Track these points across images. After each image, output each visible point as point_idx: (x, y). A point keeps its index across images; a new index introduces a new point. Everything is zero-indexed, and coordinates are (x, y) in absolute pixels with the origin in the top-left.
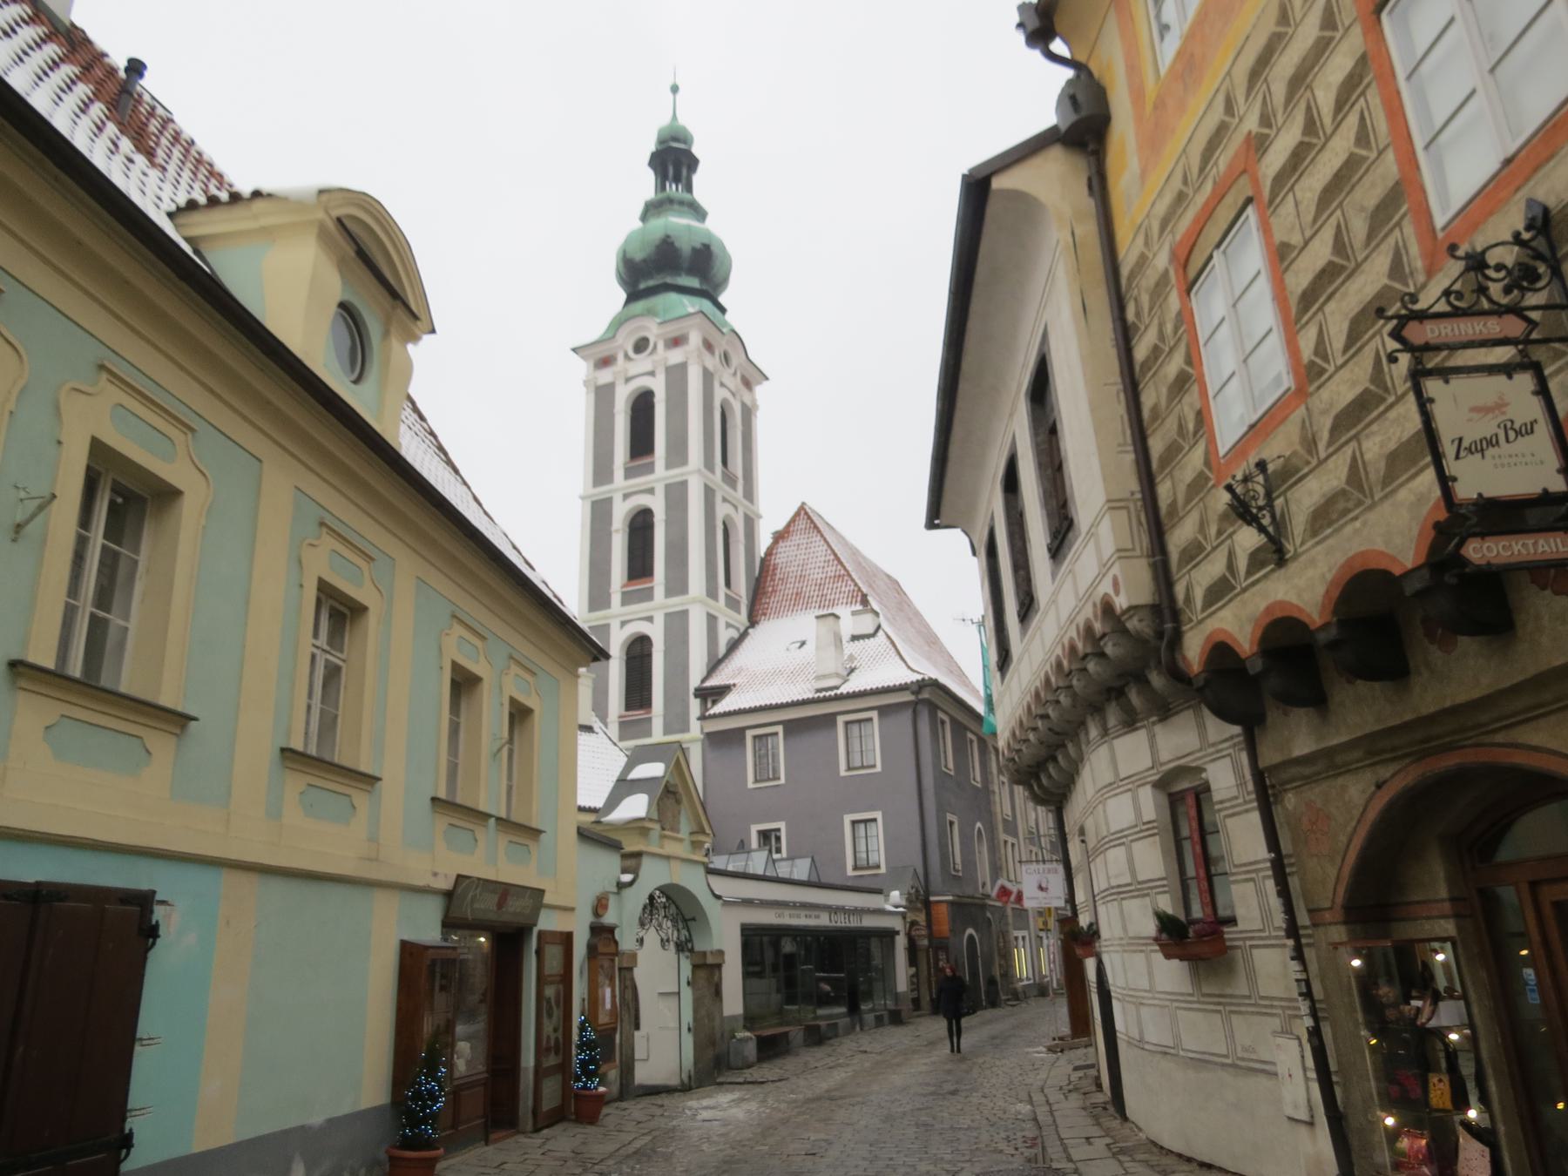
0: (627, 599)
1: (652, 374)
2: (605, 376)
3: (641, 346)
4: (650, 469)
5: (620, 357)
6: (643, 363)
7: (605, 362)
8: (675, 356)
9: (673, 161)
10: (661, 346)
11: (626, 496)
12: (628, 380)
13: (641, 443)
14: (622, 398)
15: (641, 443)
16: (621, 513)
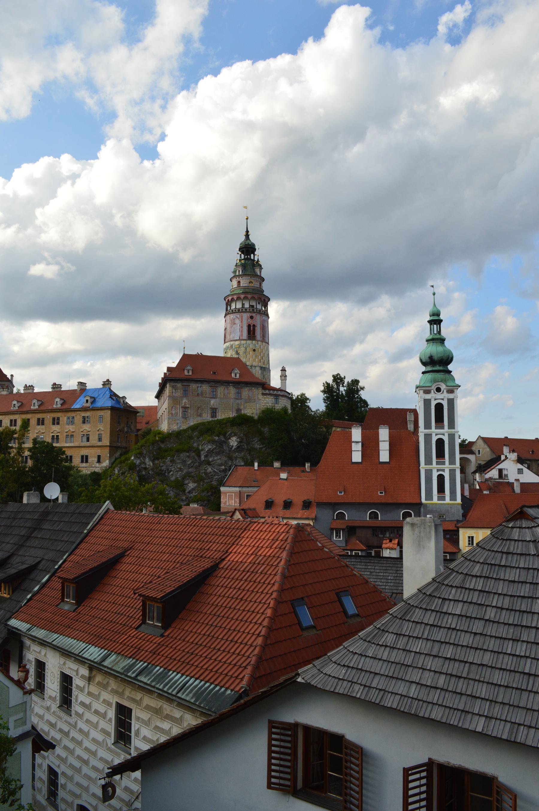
0: (438, 463)
1: (443, 399)
2: (428, 397)
3: (438, 390)
4: (443, 428)
5: (432, 391)
6: (439, 395)
7: (427, 392)
8: (451, 396)
9: (436, 321)
10: (445, 391)
11: (436, 435)
12: (435, 399)
13: (439, 419)
14: (433, 403)
15: (439, 419)
16: (434, 439)
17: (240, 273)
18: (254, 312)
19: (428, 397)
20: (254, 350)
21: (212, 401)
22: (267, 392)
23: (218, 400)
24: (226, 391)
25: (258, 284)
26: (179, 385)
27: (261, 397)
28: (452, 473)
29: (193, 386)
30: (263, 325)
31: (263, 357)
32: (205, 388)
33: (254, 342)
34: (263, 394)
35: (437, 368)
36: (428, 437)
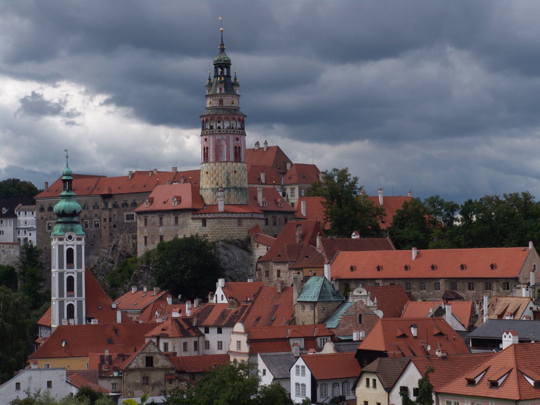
17: (223, 91)
18: (207, 135)
19: (61, 243)
20: (207, 173)
21: (161, 229)
22: (196, 216)
23: (163, 227)
24: (169, 219)
25: (218, 102)
26: (142, 217)
27: (191, 221)
28: (80, 303)
29: (150, 217)
30: (216, 145)
31: (215, 178)
32: (156, 219)
33: (207, 164)
34: (193, 219)
35: (60, 220)
36: (61, 275)
